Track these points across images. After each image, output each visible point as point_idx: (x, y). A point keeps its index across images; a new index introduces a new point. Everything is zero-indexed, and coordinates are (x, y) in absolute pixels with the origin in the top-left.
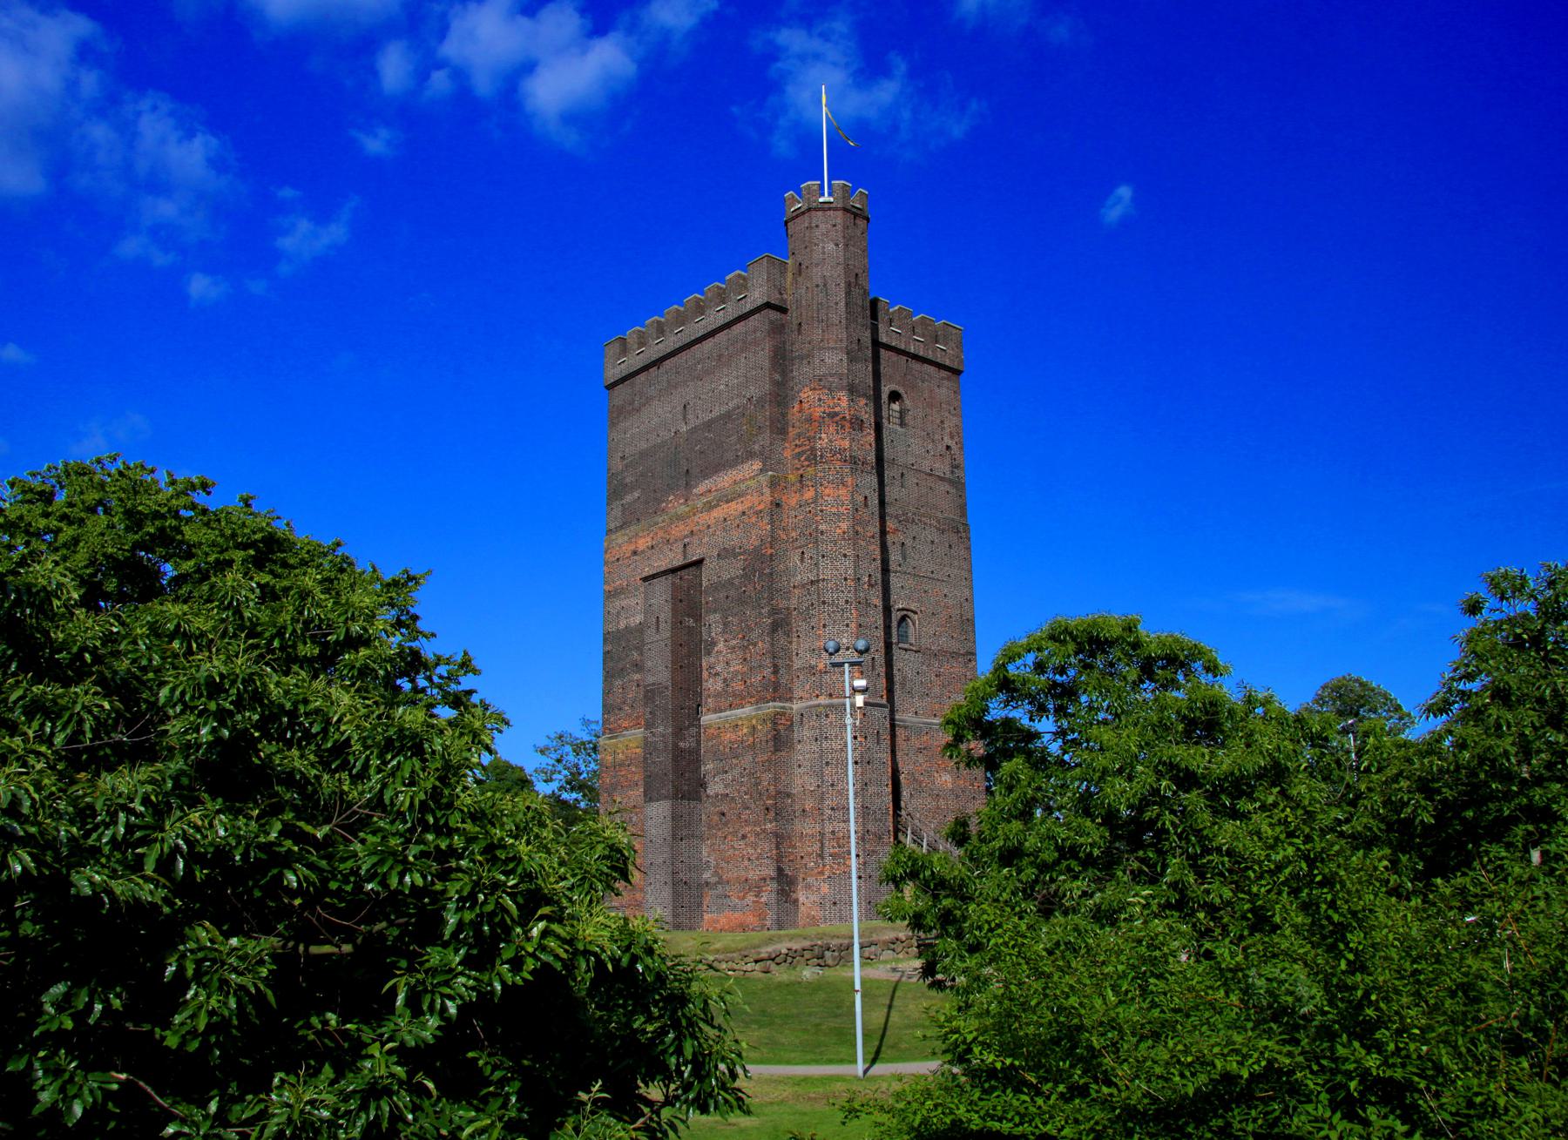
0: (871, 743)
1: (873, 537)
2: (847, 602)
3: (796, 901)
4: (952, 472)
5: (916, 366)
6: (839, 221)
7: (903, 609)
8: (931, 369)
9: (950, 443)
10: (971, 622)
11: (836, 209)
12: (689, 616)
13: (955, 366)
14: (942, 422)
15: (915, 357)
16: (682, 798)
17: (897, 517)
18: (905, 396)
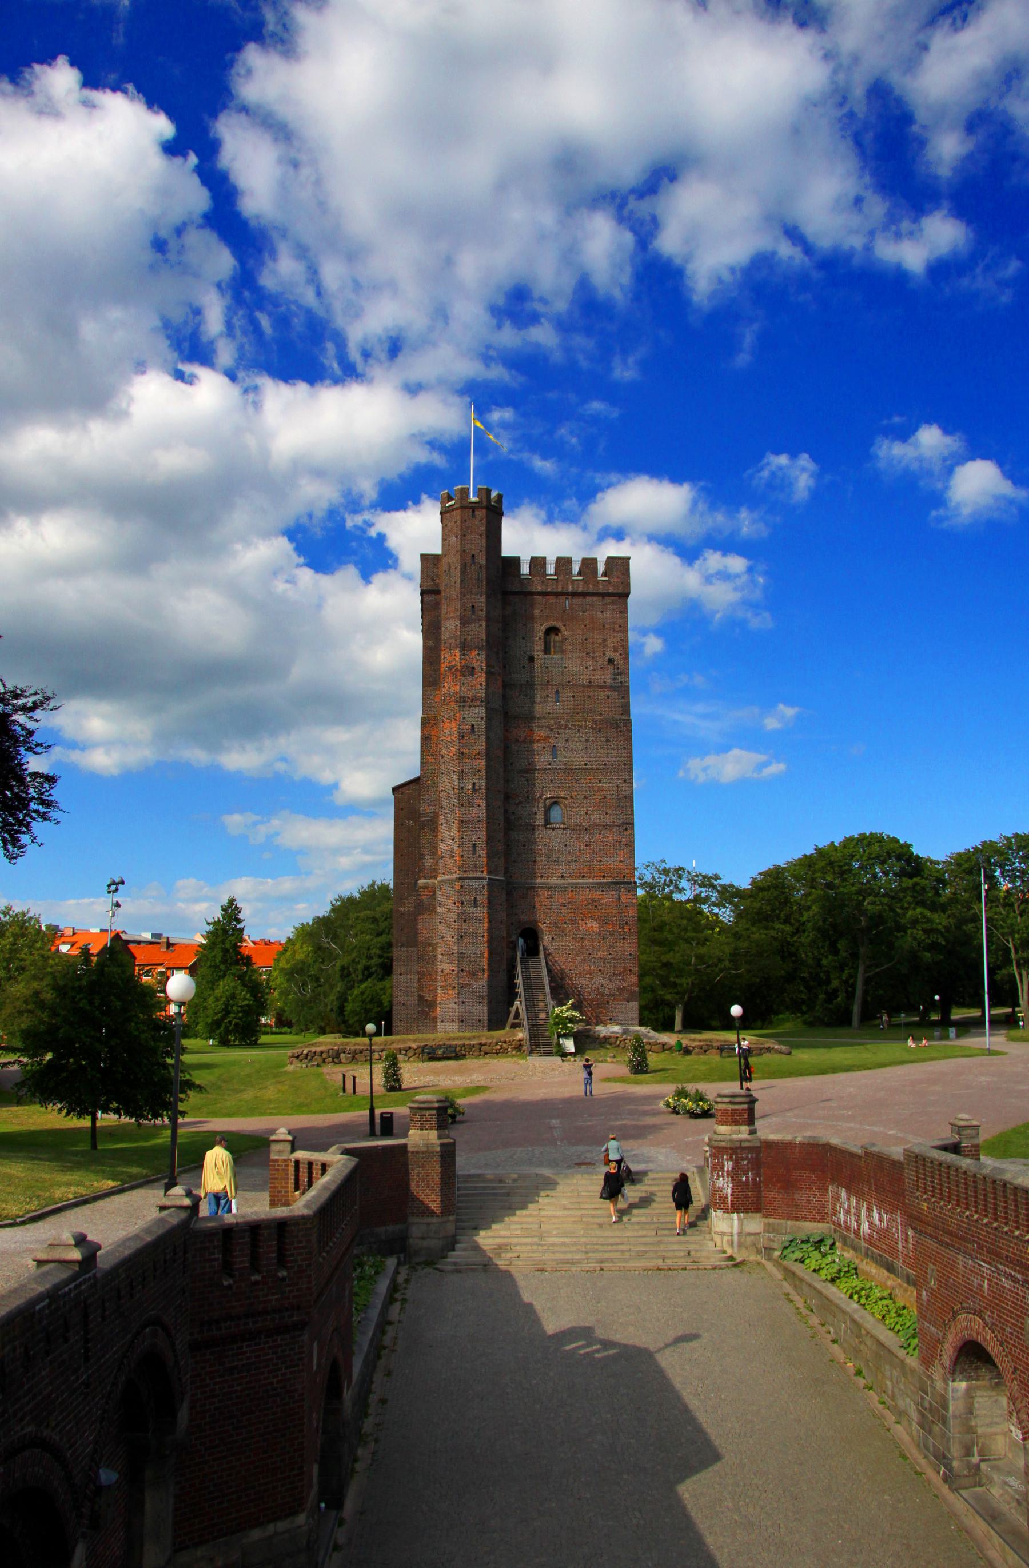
0: (469, 907)
1: (479, 754)
2: (454, 805)
3: (435, 1019)
4: (614, 679)
5: (577, 600)
6: (458, 518)
7: (551, 798)
8: (595, 599)
9: (612, 655)
10: (630, 798)
11: (457, 509)
12: (408, 819)
13: (620, 590)
14: (605, 640)
15: (574, 594)
16: (402, 946)
17: (548, 727)
18: (563, 629)
